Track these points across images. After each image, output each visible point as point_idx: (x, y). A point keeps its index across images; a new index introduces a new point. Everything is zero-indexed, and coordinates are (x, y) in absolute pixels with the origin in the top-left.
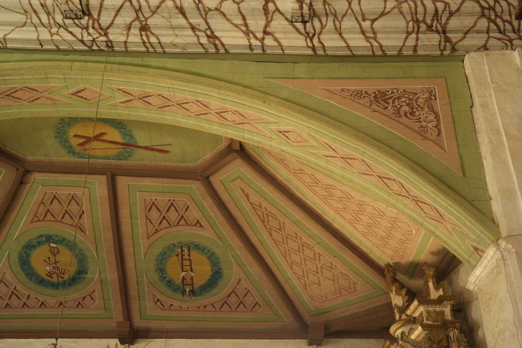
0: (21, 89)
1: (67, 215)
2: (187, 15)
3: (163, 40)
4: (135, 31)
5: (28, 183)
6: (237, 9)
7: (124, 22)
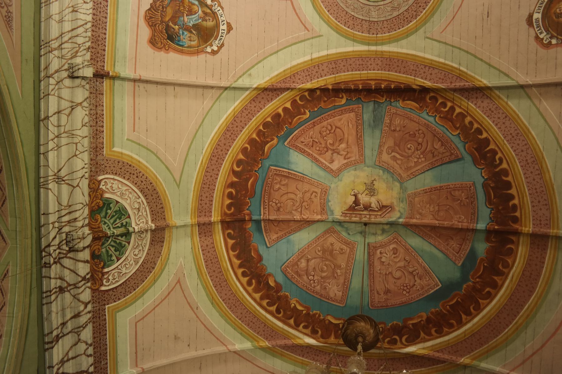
0: (3, 194)
2: (73, 319)
3: (54, 305)
4: (59, 283)
6: (80, 353)
7: (65, 275)
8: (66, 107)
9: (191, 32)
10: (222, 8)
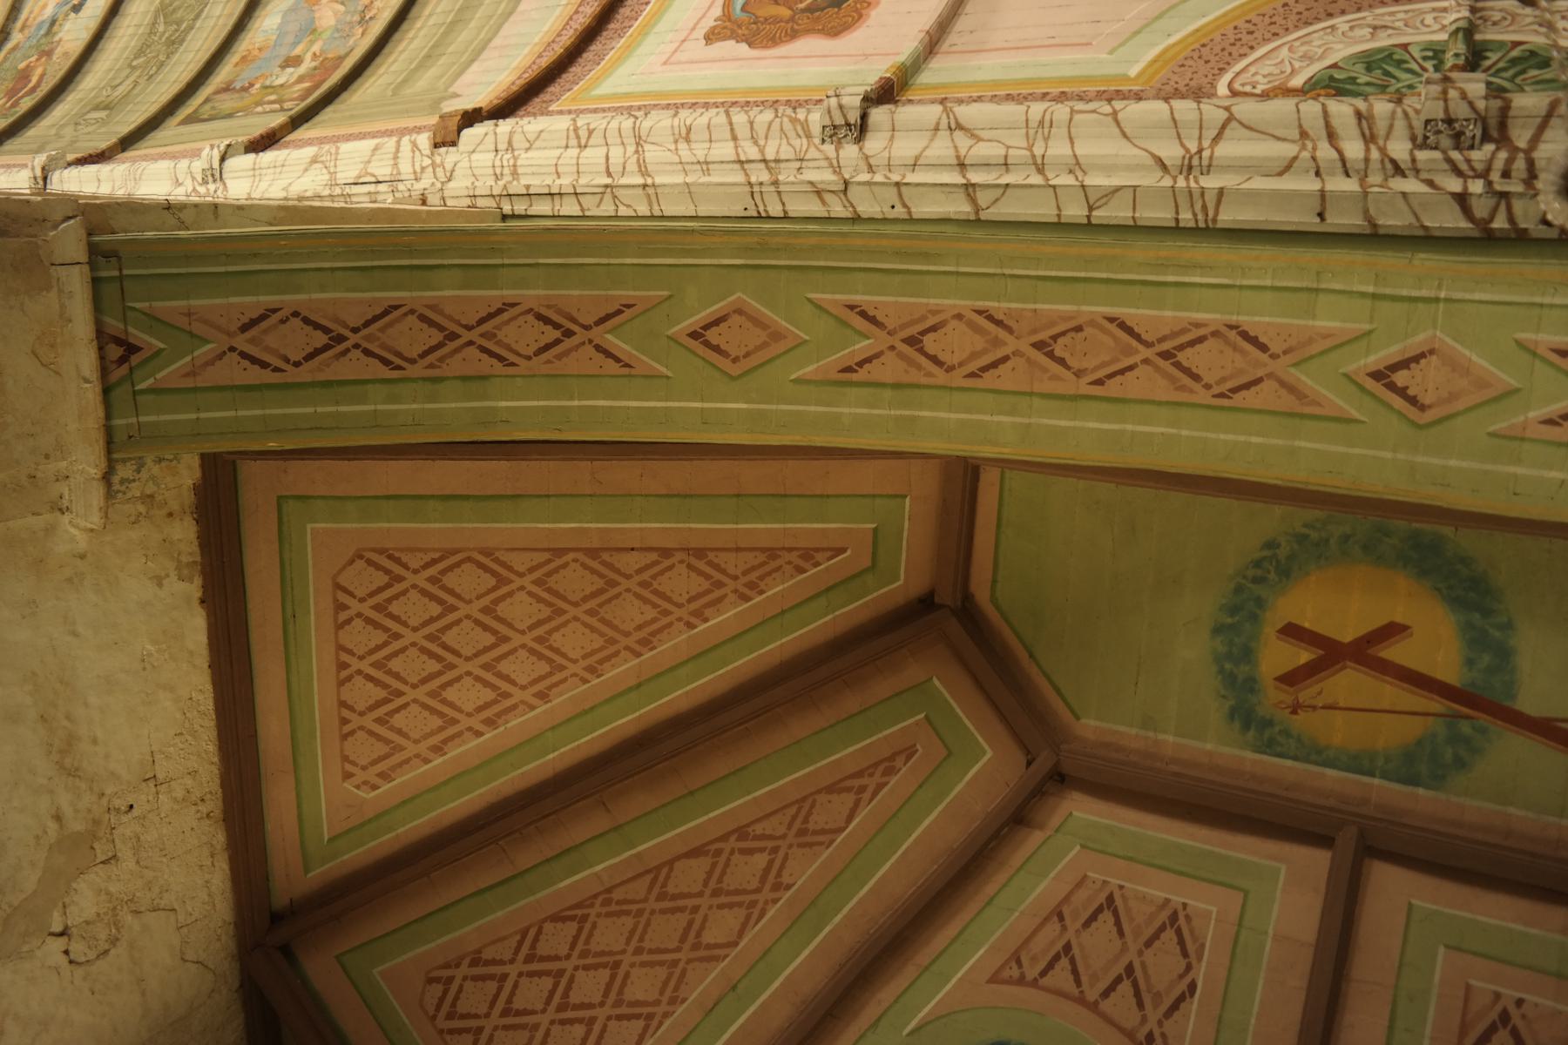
0: (1215, 334)
1: (1125, 987)
5: (1041, 827)
8: (951, 145)
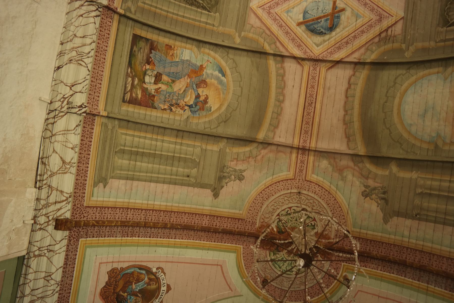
9: (137, 296)
10: (165, 274)
